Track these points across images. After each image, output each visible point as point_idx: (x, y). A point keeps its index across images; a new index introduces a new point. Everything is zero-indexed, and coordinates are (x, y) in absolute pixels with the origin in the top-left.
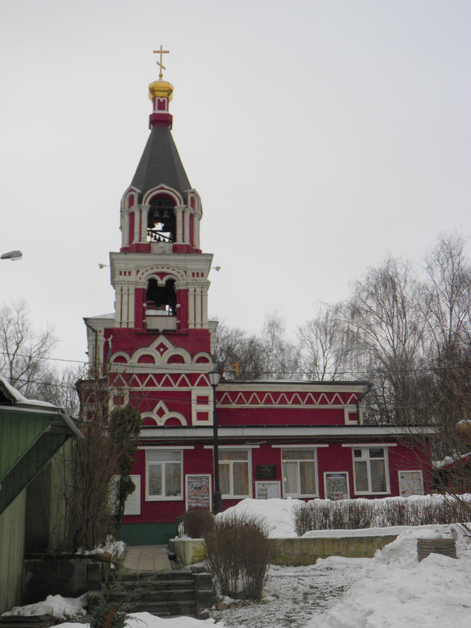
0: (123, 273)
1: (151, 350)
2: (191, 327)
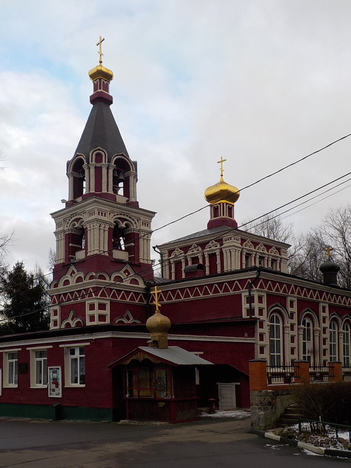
2: (142, 261)
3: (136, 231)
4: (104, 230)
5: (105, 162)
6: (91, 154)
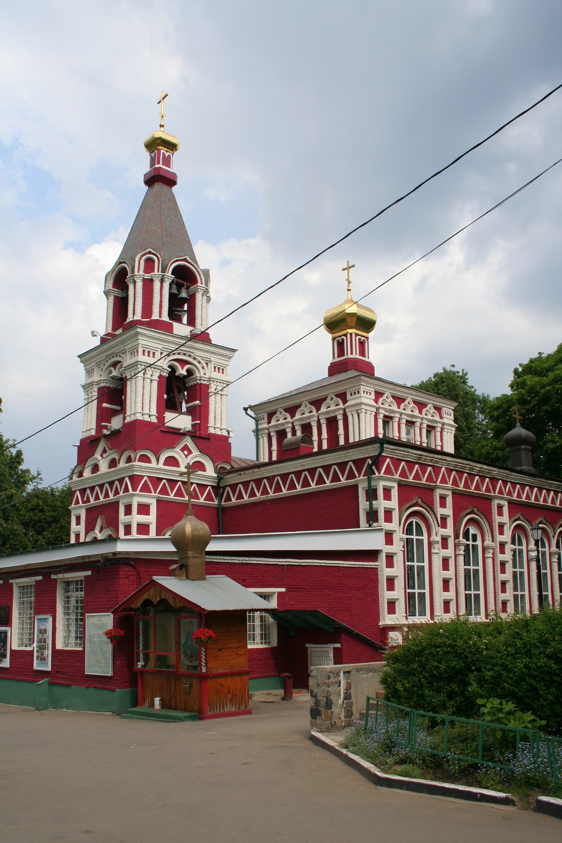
0: (146, 353)
1: (176, 453)
2: (211, 431)
3: (205, 380)
4: (151, 380)
5: (158, 272)
6: (137, 259)
